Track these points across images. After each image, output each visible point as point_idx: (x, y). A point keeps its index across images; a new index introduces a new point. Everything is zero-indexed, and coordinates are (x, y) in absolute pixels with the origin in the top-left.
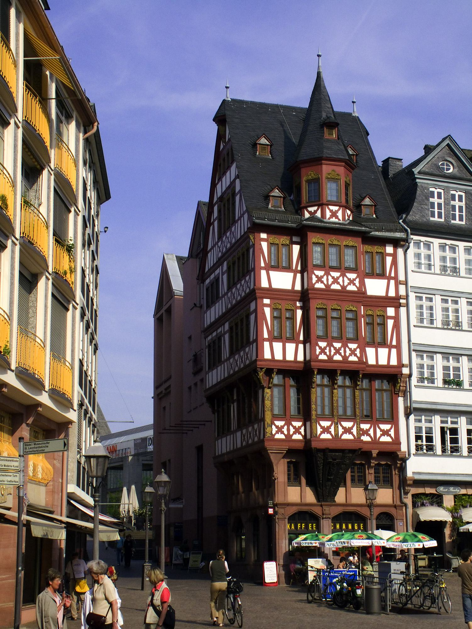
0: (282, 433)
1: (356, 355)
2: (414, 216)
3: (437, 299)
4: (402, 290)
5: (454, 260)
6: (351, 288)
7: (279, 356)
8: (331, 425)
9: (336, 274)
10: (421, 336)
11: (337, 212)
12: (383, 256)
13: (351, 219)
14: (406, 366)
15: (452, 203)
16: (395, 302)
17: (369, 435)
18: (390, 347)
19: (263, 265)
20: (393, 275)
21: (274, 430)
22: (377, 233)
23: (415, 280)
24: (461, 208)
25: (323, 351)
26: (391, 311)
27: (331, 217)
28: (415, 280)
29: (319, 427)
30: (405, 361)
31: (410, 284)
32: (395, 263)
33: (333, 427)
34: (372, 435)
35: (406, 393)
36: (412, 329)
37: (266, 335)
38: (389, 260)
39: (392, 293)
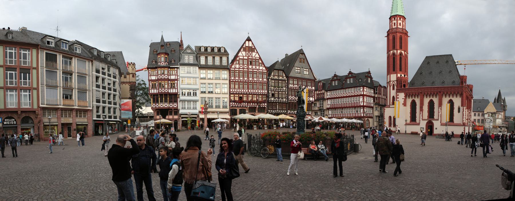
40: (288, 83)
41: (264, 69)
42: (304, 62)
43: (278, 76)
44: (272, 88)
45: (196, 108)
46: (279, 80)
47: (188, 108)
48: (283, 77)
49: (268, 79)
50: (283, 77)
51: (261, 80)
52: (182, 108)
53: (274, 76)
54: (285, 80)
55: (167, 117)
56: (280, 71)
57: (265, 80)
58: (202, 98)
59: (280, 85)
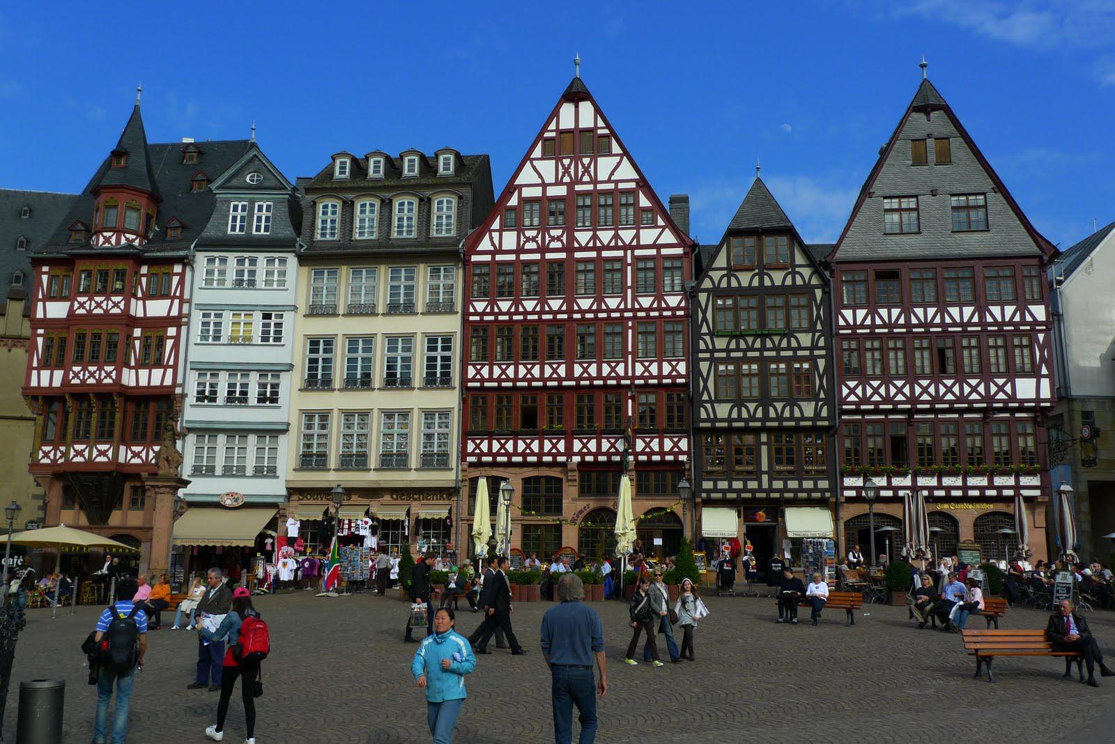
0: (48, 457)
1: (111, 377)
2: (210, 231)
3: (228, 317)
4: (185, 310)
5: (252, 273)
6: (116, 311)
7: (45, 383)
8: (86, 448)
9: (98, 299)
10: (200, 354)
11: (110, 237)
12: (170, 275)
13: (136, 243)
14: (180, 385)
15: (245, 214)
16: (176, 321)
17: (141, 458)
18: (166, 367)
19: (40, 297)
20: (178, 294)
21: (41, 454)
22: (159, 254)
23: (201, 297)
24: (267, 219)
25: (76, 375)
26: (172, 331)
27: (104, 243)
28: (201, 297)
29: (72, 450)
30: (179, 381)
31: (195, 301)
32: (181, 282)
33: (87, 451)
34: (144, 457)
35: (180, 412)
36: (191, 346)
37: (35, 364)
38: (176, 279)
39: (175, 312)
40: (832, 307)
41: (668, 237)
42: (944, 158)
43: (763, 269)
44: (721, 343)
45: (272, 472)
46: (761, 293)
47: (228, 472)
48: (791, 268)
49: (691, 295)
50: (791, 268)
51: (646, 302)
52: (197, 471)
53: (731, 270)
54: (807, 289)
55: (116, 518)
56: (768, 240)
57: (673, 301)
58: (309, 415)
59: (775, 321)
